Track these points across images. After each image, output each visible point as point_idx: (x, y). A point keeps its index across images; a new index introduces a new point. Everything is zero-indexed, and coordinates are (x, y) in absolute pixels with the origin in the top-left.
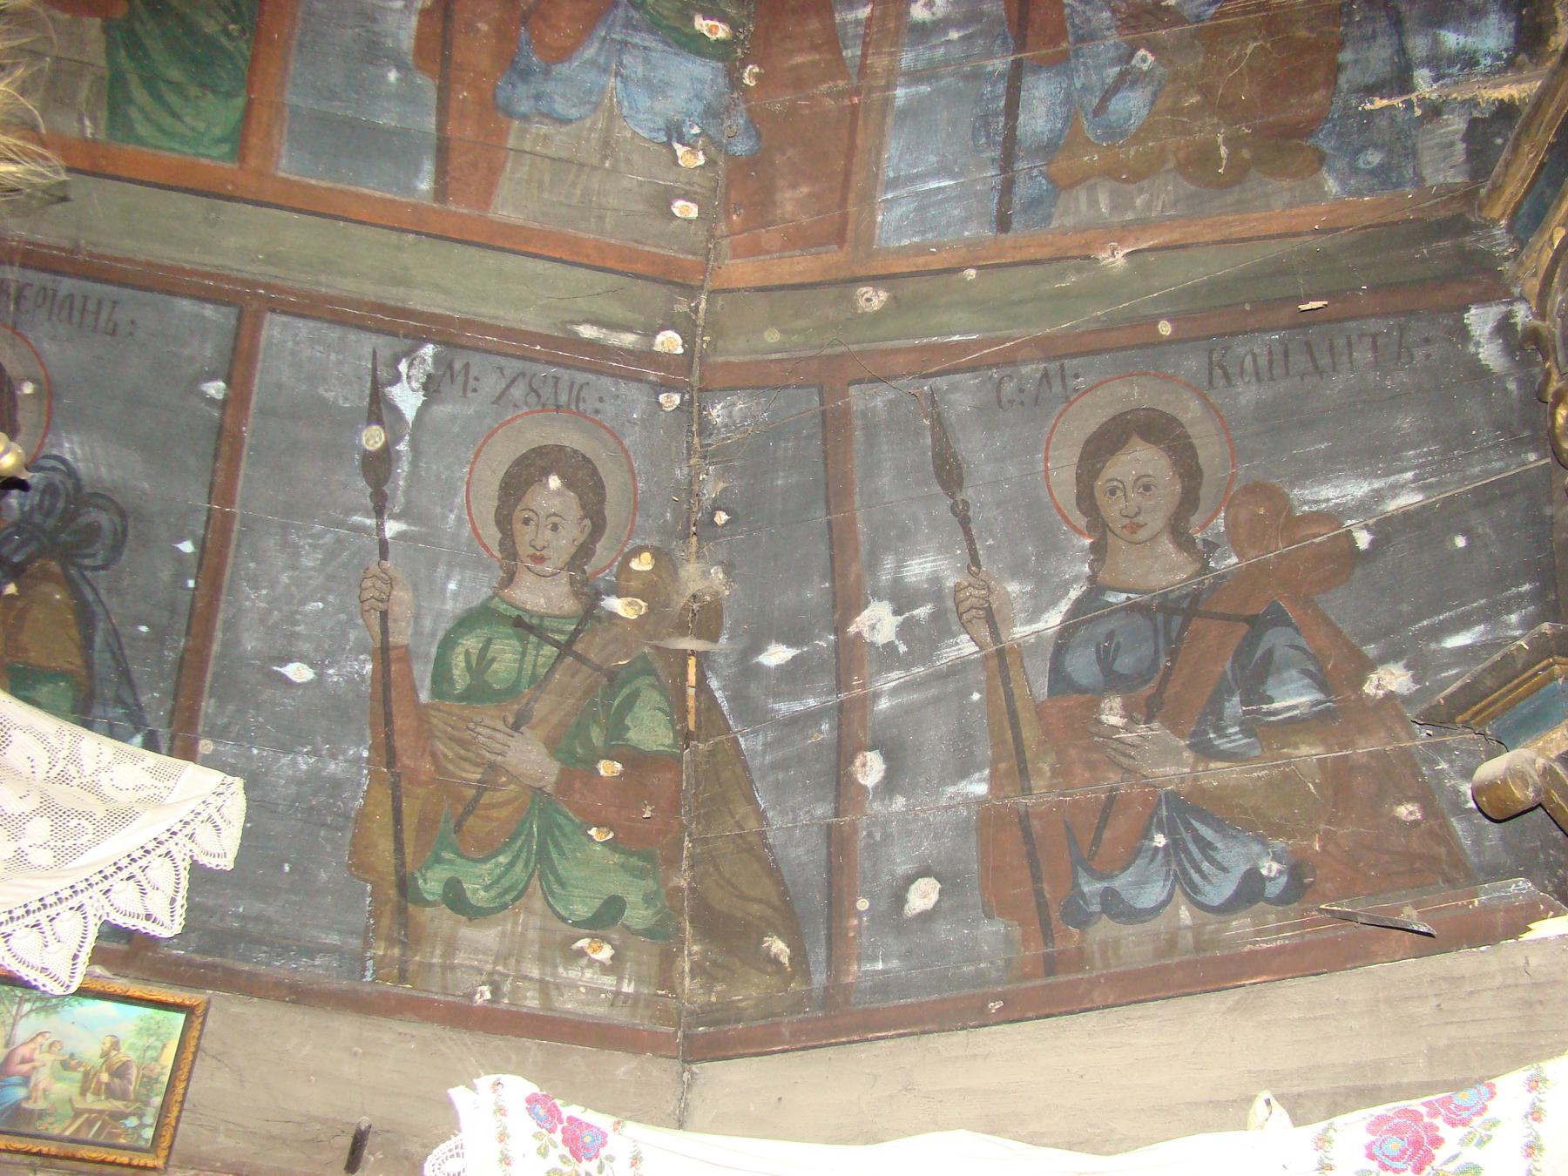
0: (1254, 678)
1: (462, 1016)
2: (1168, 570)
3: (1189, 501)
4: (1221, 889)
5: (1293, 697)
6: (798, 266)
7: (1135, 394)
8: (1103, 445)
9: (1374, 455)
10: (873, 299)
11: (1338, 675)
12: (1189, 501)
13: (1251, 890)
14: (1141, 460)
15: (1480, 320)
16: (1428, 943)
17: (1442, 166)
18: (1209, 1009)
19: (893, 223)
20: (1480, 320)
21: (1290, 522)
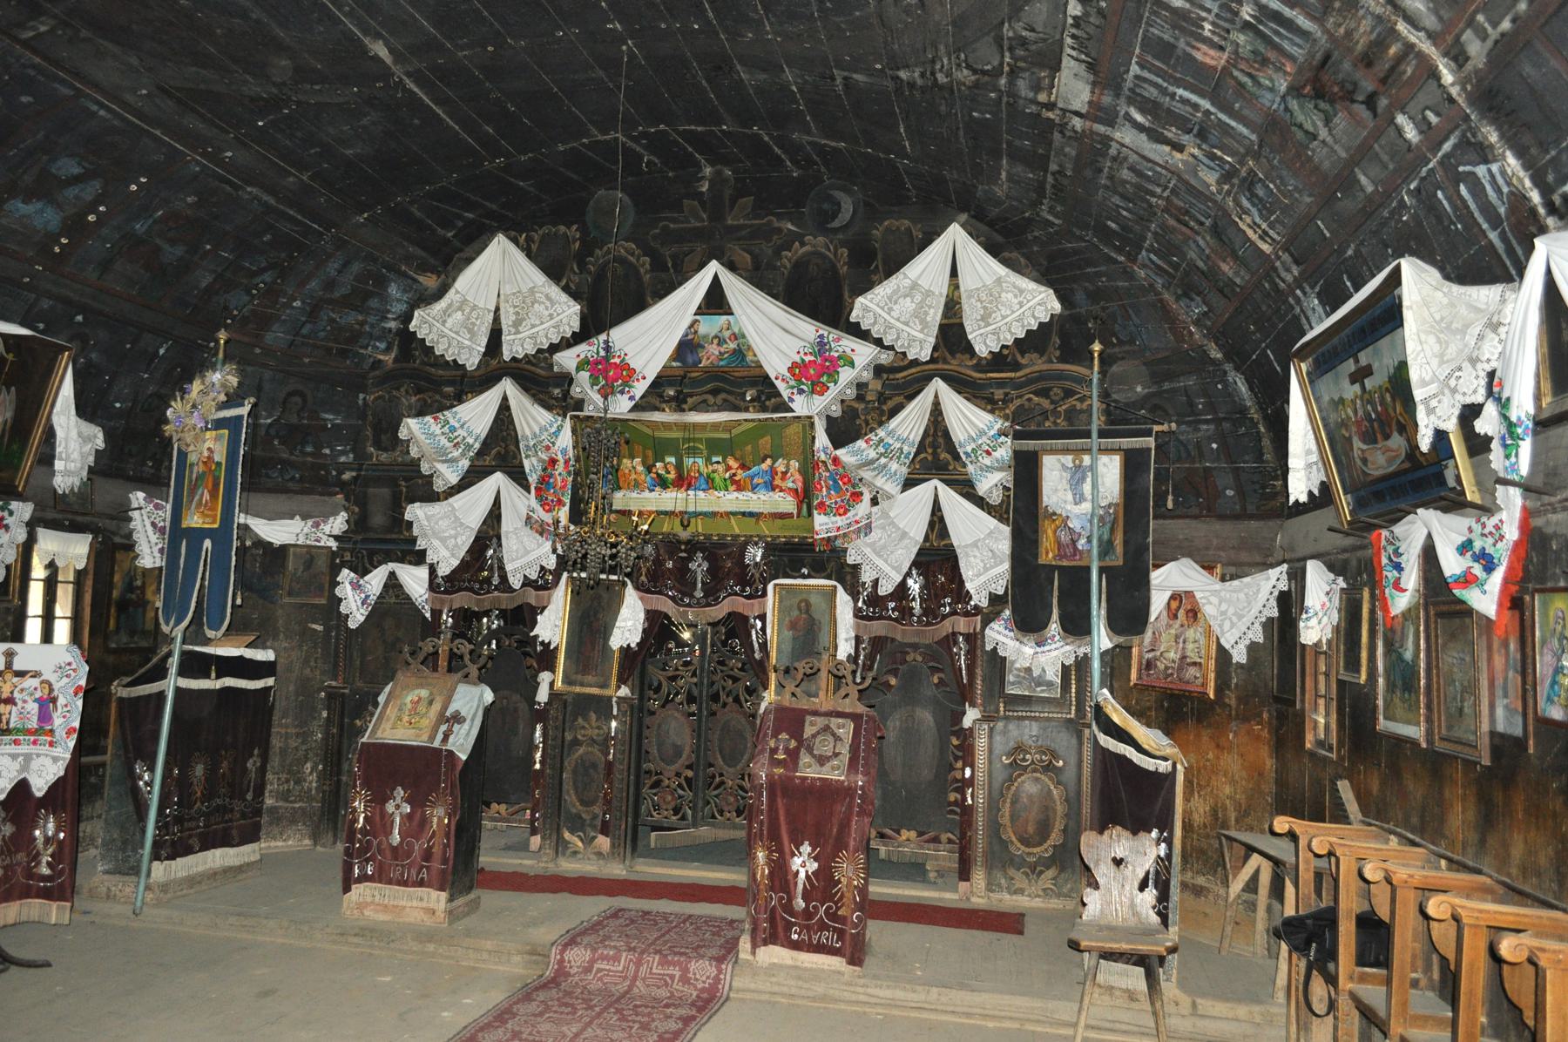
0: (304, 443)
1: (129, 479)
2: (294, 420)
3: (302, 409)
4: (287, 477)
5: (309, 449)
6: (246, 339)
7: (300, 387)
8: (290, 394)
9: (336, 413)
10: (258, 351)
11: (319, 447)
12: (302, 409)
13: (293, 478)
14: (297, 399)
15: (361, 396)
16: (322, 494)
17: (366, 367)
18: (283, 497)
19: (269, 338)
20: (361, 396)
21: (318, 418)
